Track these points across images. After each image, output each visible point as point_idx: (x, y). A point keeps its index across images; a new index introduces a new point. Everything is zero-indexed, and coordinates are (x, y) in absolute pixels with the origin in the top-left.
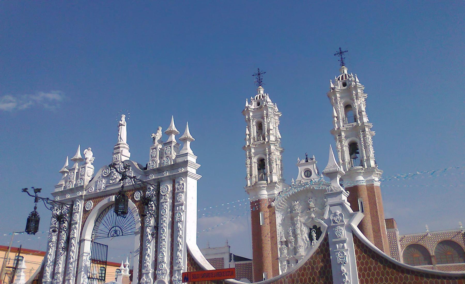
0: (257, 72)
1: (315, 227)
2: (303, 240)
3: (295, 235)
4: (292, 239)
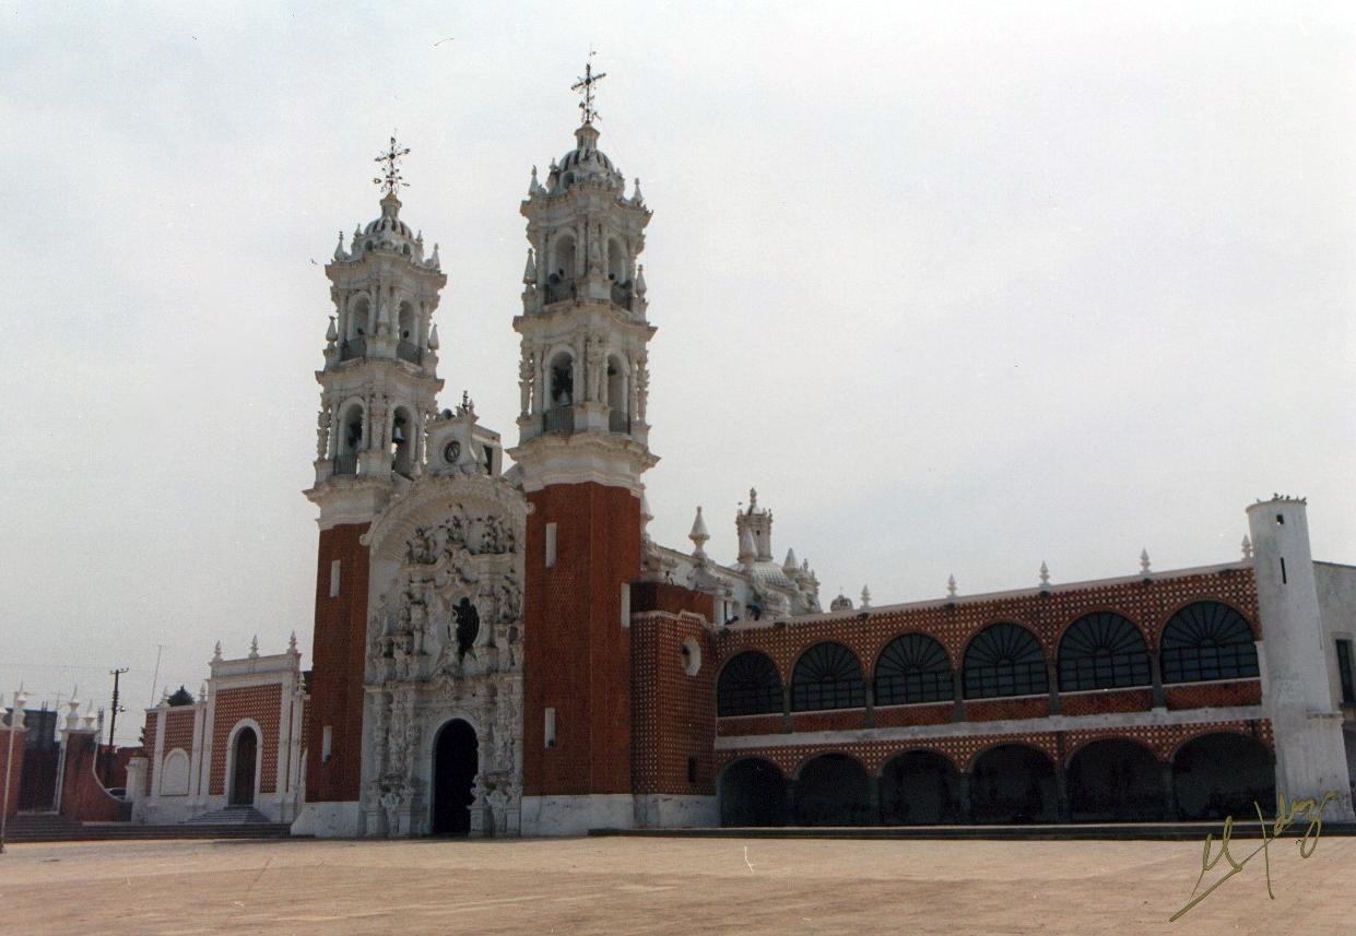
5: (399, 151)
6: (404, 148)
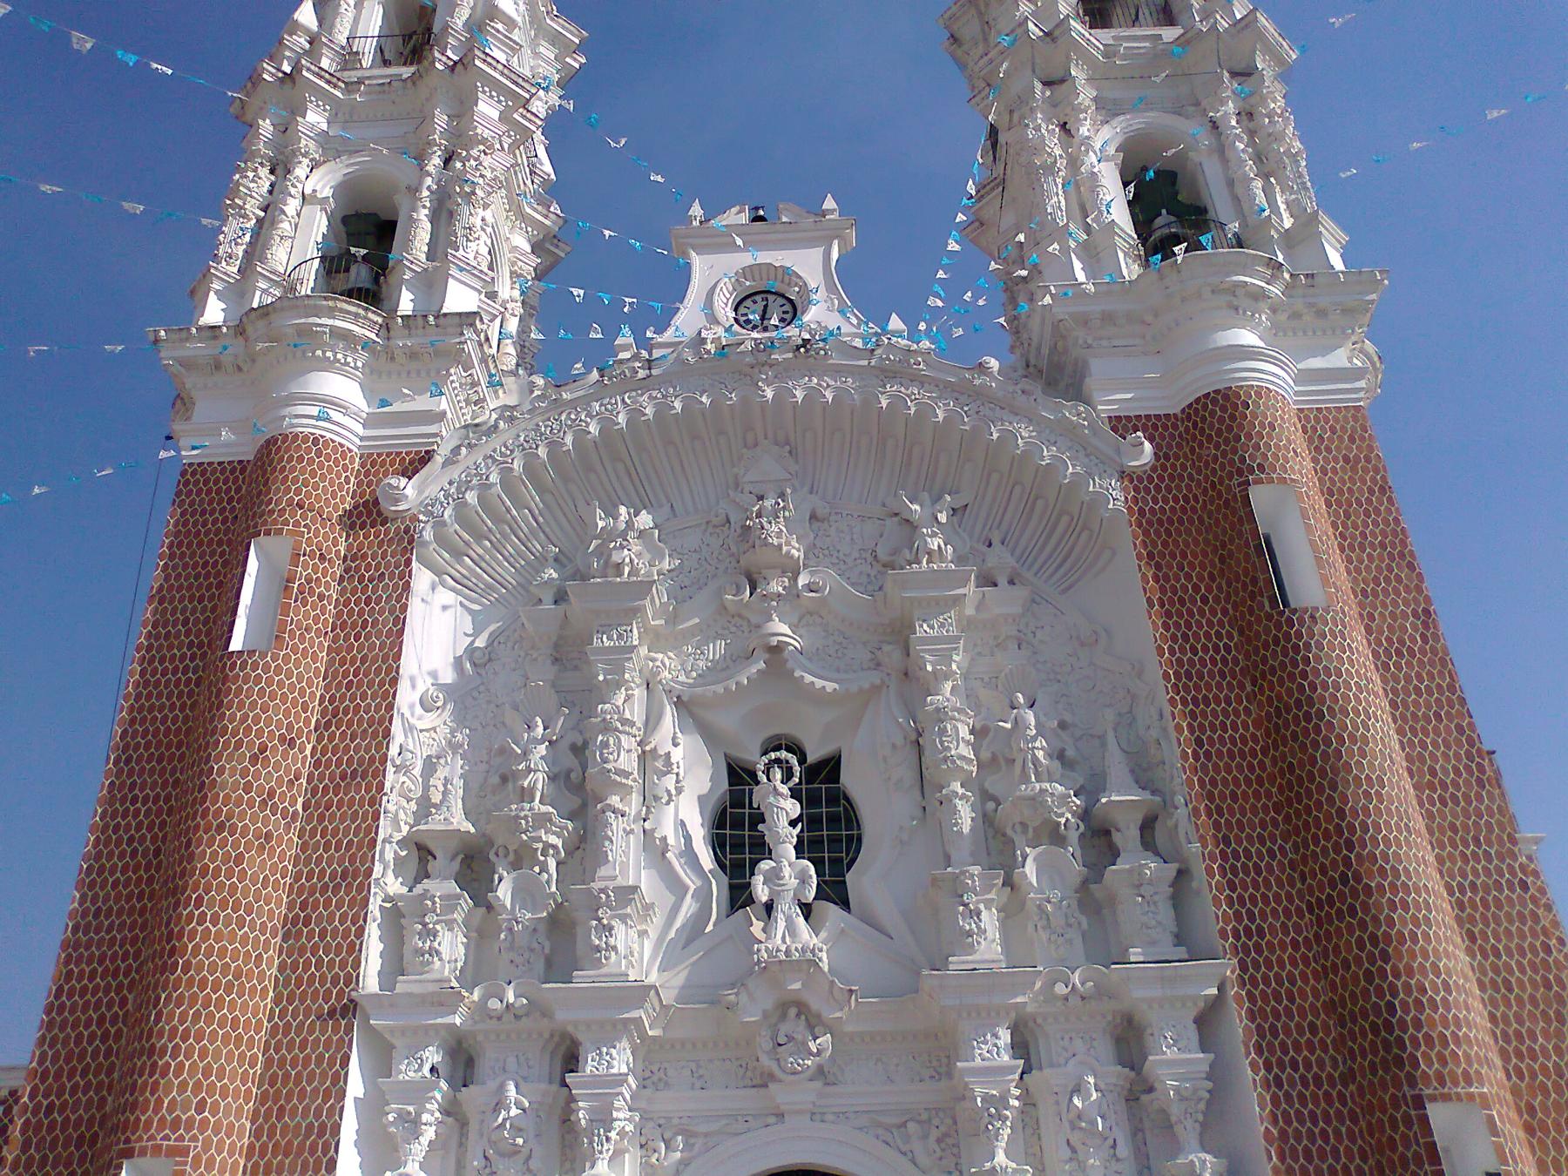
2: (655, 849)
3: (581, 792)
4: (542, 820)
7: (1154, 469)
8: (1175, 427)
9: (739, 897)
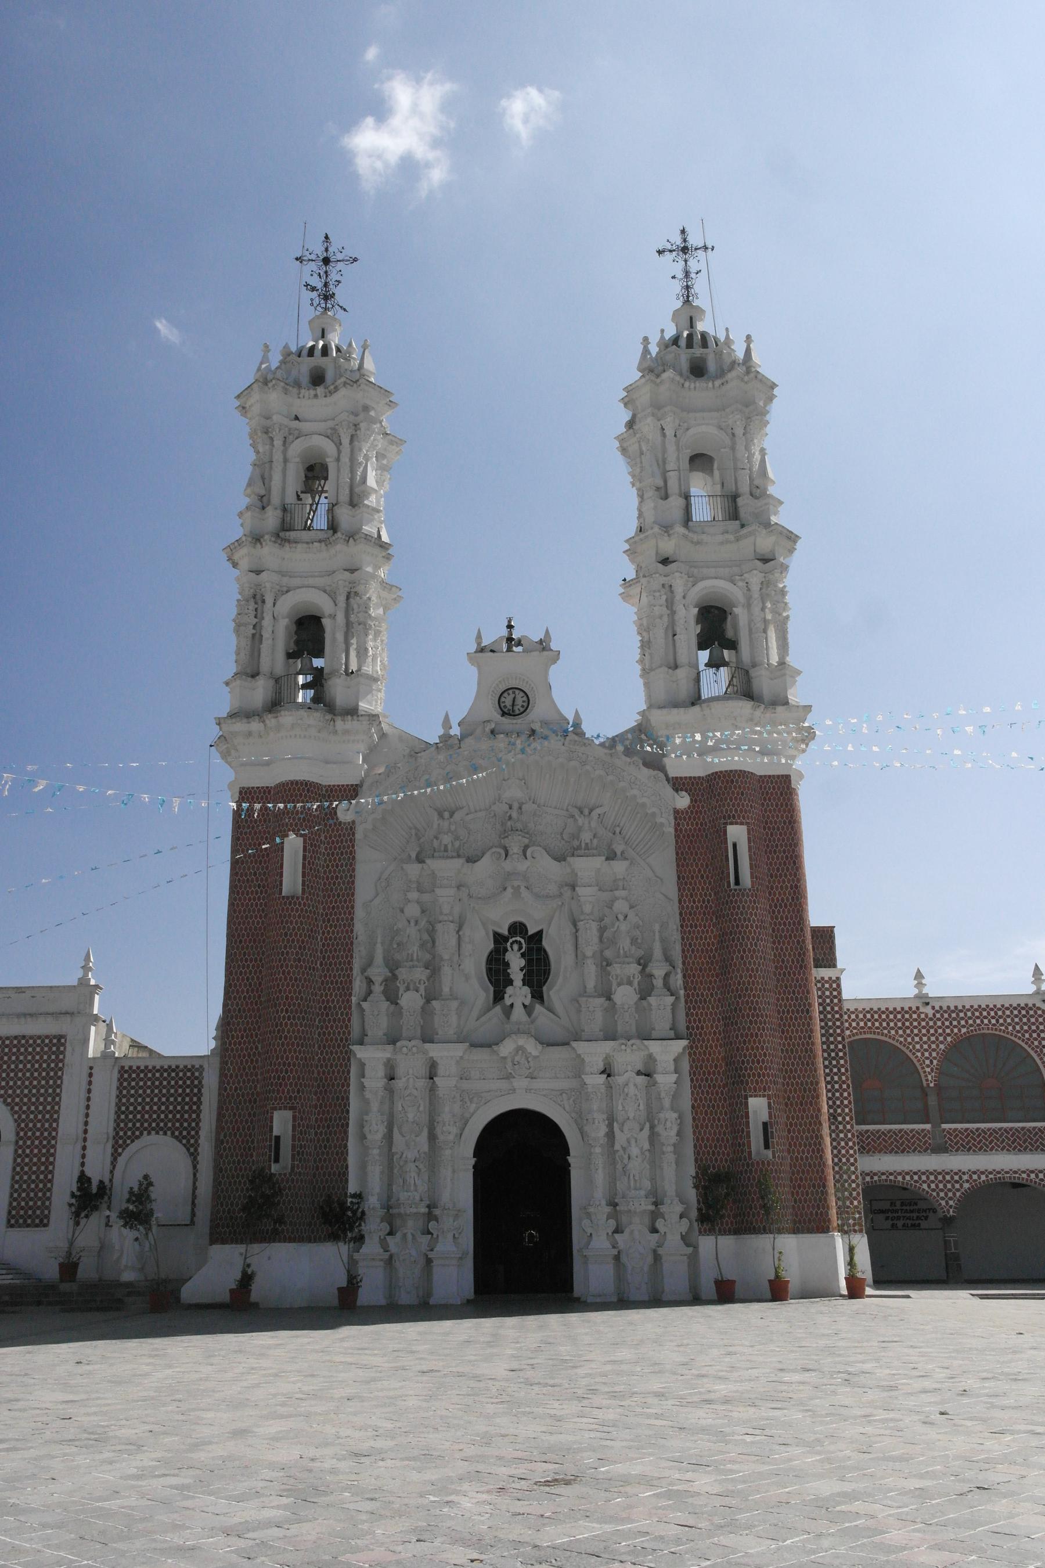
0: (319, 250)
1: (517, 928)
5: (340, 257)
6: (349, 253)
7: (689, 807)
8: (702, 784)
9: (499, 997)
